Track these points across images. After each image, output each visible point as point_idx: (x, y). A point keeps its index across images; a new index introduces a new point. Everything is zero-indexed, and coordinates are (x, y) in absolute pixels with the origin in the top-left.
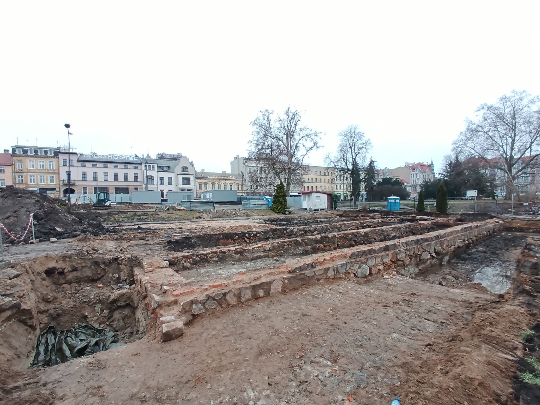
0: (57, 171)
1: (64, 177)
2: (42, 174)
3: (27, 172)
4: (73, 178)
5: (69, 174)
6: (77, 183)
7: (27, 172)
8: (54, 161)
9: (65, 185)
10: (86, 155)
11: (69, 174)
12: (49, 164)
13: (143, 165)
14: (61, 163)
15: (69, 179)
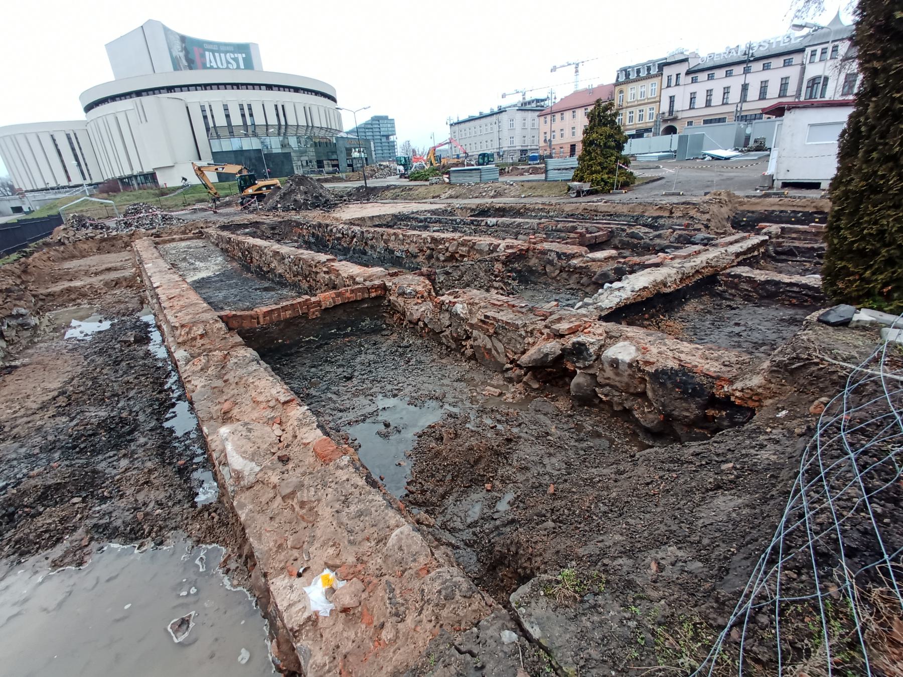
0: (657, 99)
1: (665, 107)
2: (641, 108)
3: (627, 107)
4: (677, 107)
5: (672, 99)
6: (680, 116)
7: (627, 107)
8: (656, 81)
9: (665, 121)
10: (720, 54)
11: (672, 99)
12: (648, 88)
13: (808, 51)
14: (665, 84)
15: (671, 112)
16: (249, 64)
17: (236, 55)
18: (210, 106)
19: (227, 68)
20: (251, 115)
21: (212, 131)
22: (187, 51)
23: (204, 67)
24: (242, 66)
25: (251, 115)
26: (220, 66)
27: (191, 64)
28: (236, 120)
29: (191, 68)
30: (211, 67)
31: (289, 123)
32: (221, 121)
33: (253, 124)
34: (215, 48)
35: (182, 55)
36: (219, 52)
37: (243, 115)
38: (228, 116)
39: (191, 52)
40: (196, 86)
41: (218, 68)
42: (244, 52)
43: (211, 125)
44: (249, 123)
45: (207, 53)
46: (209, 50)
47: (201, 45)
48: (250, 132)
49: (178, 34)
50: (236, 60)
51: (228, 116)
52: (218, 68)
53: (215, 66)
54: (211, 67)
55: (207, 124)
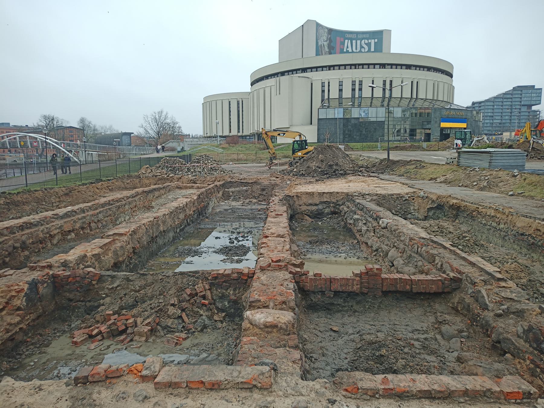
16: (379, 48)
17: (370, 41)
18: (329, 82)
19: (360, 51)
20: (360, 89)
21: (326, 102)
22: (330, 40)
23: (342, 52)
24: (373, 49)
25: (360, 89)
26: (354, 50)
27: (331, 51)
28: (347, 93)
29: (330, 53)
30: (347, 52)
31: (393, 96)
32: (334, 94)
33: (360, 97)
34: (354, 36)
35: (326, 43)
36: (356, 40)
37: (353, 90)
38: (341, 90)
39: (334, 40)
40: (322, 67)
41: (353, 52)
42: (378, 37)
43: (326, 97)
44: (357, 96)
45: (346, 41)
46: (348, 39)
47: (343, 34)
48: (356, 104)
49: (327, 28)
50: (369, 45)
51: (341, 90)
52: (353, 52)
53: (350, 51)
54: (347, 52)
55: (323, 96)
